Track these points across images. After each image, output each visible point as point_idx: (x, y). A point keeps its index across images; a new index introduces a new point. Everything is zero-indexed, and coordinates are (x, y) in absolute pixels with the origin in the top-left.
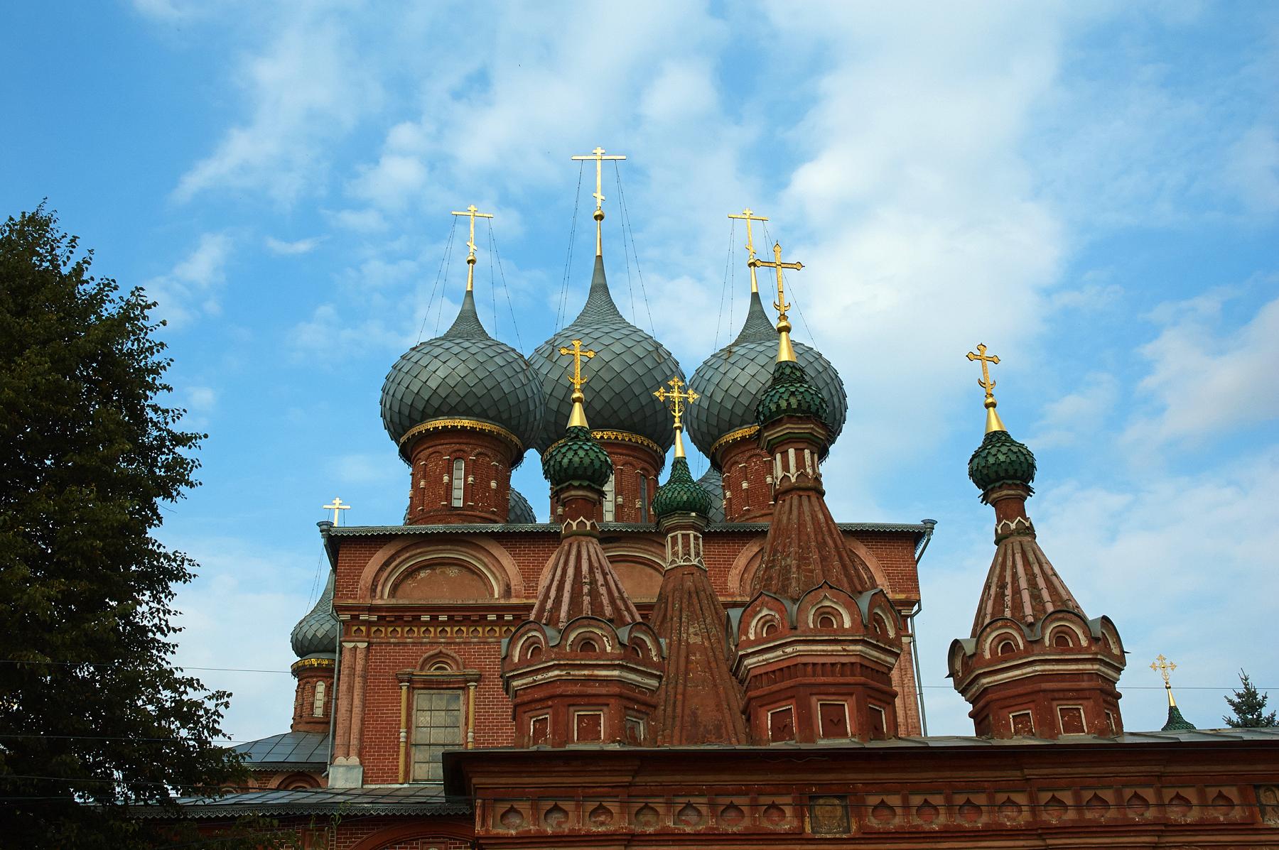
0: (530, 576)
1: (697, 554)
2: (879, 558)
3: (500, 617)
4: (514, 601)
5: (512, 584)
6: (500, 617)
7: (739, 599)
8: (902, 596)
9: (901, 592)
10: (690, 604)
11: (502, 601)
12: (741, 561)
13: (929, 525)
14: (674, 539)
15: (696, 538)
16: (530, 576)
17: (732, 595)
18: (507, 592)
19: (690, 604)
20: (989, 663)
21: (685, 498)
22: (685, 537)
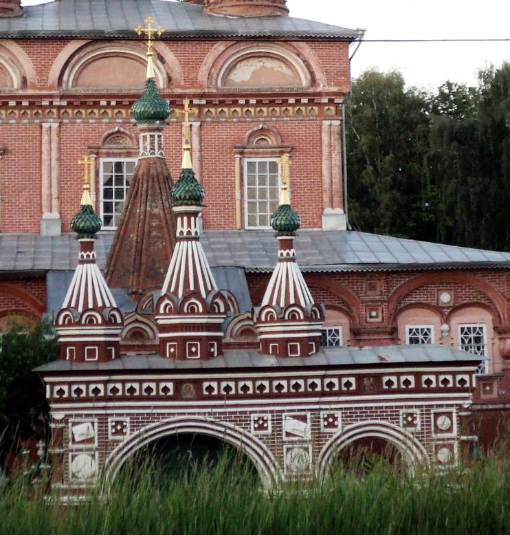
0: (42, 69)
1: (160, 148)
2: (320, 57)
3: (19, 104)
4: (30, 92)
5: (28, 78)
6: (19, 104)
7: (206, 91)
8: (334, 89)
9: (336, 85)
10: (153, 187)
11: (21, 92)
12: (210, 59)
13: (361, 32)
14: (145, 137)
15: (159, 136)
16: (42, 69)
17: (201, 87)
18: (24, 81)
19: (153, 187)
20: (263, 323)
21: (152, 112)
22: (152, 136)
